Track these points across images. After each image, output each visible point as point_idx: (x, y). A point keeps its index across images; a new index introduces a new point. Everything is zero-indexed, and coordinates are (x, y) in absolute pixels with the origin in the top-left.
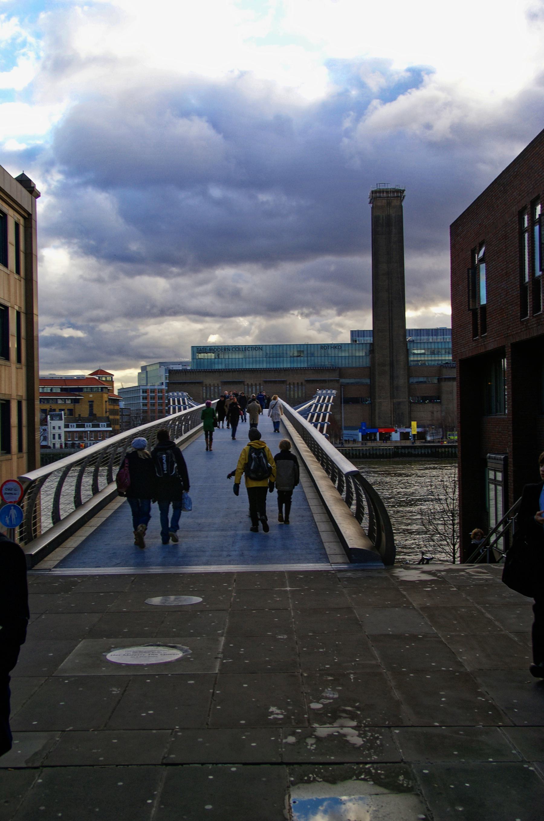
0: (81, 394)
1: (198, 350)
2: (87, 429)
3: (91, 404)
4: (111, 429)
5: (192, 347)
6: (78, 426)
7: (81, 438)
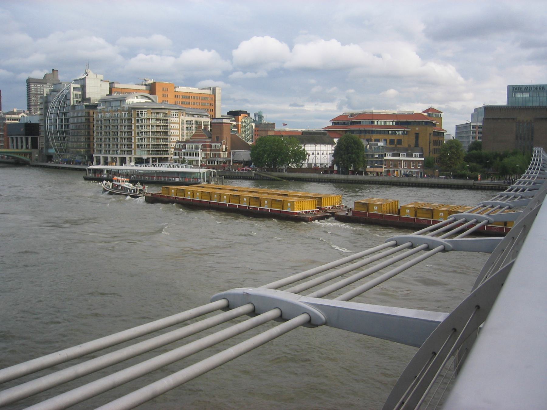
0: (409, 127)
1: (513, 90)
2: (401, 158)
3: (417, 135)
4: (423, 159)
5: (509, 87)
6: (393, 155)
7: (395, 166)
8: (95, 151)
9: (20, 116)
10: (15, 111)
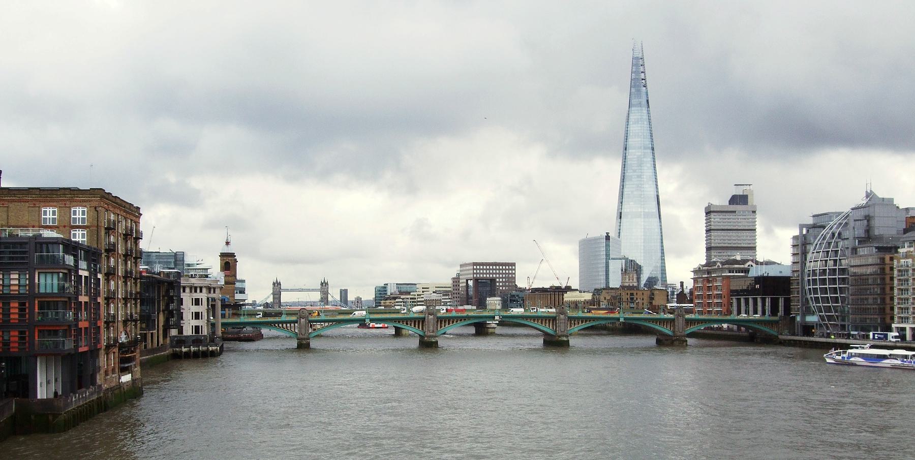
8: (896, 319)
9: (746, 266)
10: (738, 258)
